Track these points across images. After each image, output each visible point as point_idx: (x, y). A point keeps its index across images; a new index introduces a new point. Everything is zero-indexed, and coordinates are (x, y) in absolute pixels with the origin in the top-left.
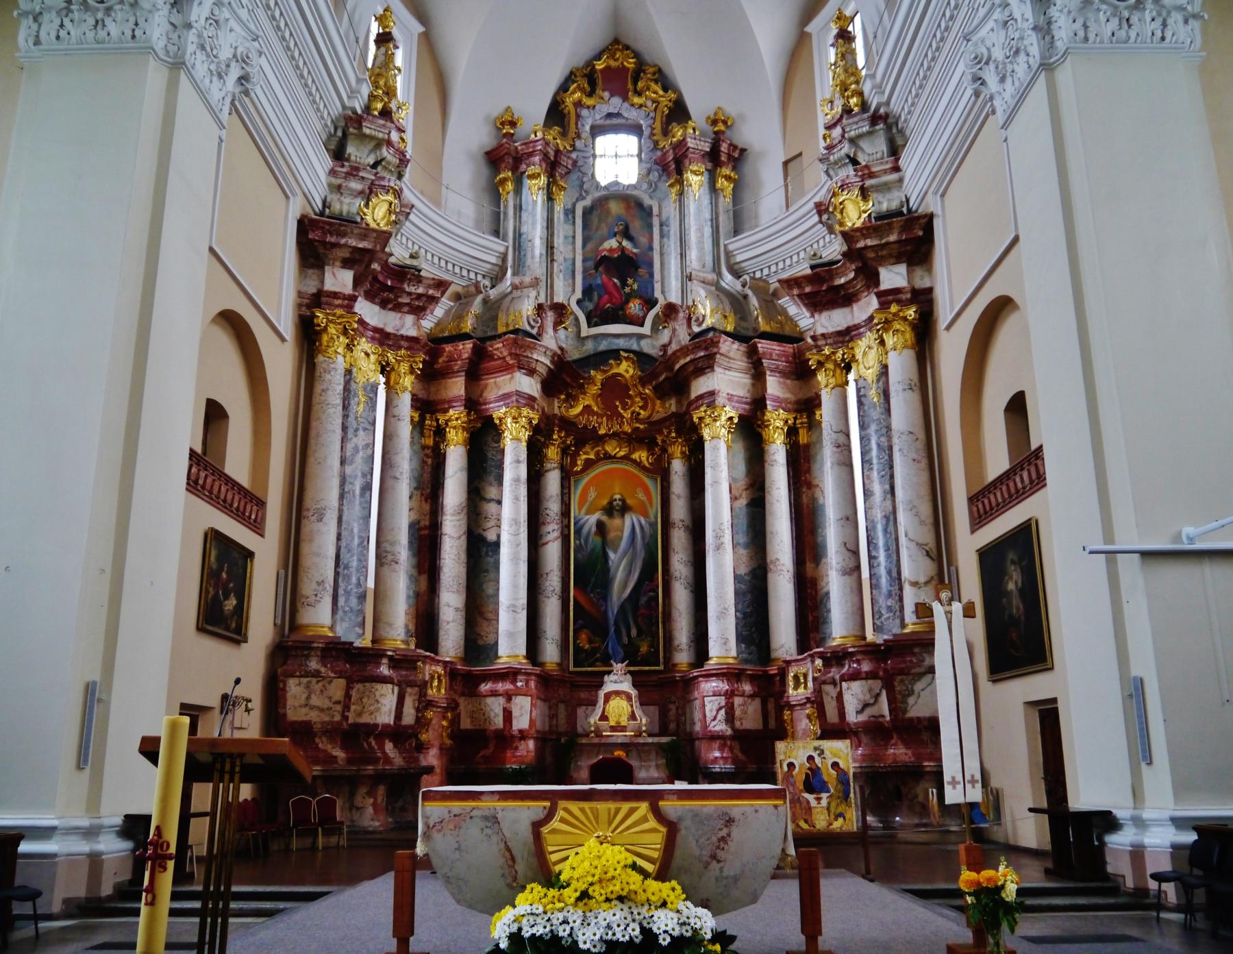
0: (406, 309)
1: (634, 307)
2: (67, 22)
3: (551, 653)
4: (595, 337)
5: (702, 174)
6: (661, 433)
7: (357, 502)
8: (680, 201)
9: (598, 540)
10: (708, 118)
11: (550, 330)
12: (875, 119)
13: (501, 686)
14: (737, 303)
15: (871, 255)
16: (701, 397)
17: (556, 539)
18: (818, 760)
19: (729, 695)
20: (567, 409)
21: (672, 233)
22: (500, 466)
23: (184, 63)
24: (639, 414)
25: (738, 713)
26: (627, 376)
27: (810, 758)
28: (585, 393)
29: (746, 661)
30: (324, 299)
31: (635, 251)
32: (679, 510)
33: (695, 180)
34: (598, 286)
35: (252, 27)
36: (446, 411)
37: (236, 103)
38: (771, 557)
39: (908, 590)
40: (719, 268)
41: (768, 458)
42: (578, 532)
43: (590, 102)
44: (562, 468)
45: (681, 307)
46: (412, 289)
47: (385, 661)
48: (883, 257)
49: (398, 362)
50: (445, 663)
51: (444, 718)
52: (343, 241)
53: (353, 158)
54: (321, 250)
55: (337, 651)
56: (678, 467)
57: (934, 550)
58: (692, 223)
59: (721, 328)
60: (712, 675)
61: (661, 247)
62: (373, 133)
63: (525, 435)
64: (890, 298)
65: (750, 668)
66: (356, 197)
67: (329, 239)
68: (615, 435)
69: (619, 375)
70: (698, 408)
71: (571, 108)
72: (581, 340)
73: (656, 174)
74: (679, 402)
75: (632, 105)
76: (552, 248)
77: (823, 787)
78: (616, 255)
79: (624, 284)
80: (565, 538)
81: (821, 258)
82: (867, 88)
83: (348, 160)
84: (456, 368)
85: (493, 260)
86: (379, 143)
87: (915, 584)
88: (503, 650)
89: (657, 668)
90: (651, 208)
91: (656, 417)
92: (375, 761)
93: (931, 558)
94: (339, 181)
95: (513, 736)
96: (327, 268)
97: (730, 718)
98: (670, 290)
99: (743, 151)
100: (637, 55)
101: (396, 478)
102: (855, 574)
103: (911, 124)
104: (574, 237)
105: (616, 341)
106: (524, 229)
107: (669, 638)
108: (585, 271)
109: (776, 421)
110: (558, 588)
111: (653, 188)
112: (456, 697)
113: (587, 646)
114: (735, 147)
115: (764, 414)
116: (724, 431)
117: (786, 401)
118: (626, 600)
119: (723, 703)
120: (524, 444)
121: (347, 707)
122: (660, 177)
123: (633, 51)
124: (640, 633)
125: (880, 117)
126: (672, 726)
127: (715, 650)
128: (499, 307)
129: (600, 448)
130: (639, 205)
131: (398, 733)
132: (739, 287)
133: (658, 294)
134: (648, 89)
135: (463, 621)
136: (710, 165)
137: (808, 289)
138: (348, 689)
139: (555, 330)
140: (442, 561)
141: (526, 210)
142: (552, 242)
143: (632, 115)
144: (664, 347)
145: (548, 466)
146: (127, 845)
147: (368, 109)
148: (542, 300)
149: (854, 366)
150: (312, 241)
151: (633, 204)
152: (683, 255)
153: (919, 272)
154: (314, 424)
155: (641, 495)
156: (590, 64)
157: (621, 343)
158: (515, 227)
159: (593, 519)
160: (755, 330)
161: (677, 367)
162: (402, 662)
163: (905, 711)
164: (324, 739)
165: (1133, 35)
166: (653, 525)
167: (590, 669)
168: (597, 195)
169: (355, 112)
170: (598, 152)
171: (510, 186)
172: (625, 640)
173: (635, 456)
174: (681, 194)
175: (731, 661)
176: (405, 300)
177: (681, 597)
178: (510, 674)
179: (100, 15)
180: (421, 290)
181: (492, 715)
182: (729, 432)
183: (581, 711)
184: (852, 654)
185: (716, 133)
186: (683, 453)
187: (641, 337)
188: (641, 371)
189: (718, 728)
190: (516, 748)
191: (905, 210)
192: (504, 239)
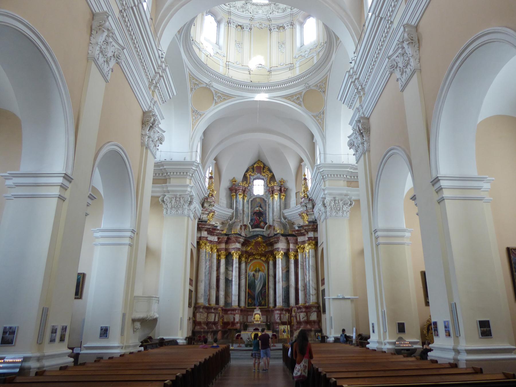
0: (215, 235)
1: (262, 224)
2: (172, 210)
3: (243, 304)
4: (253, 231)
5: (277, 195)
6: (267, 255)
7: (207, 277)
8: (273, 200)
9: (253, 278)
10: (280, 181)
11: (243, 230)
12: (309, 200)
13: (232, 312)
14: (284, 226)
15: (307, 230)
16: (276, 249)
17: (244, 278)
18: (285, 328)
19: (280, 314)
20: (247, 249)
21: (271, 207)
22: (232, 263)
23: (190, 216)
24: (263, 249)
25: (282, 318)
26: (260, 241)
27: (284, 328)
28: (251, 245)
29: (284, 306)
30: (202, 238)
31: (262, 211)
32: (271, 272)
33: (276, 197)
34: (254, 219)
35: (197, 201)
36: (221, 251)
37: (194, 216)
38: (290, 284)
39: (311, 296)
40: (281, 217)
41: (290, 262)
42: (249, 276)
43: (253, 174)
44: (245, 262)
45: (272, 225)
46: (217, 232)
47: (213, 309)
48: (309, 230)
49: (214, 247)
50: (221, 308)
51: (221, 319)
52: (205, 227)
53: (206, 207)
54: (201, 228)
55: (205, 308)
56: (271, 262)
57: (316, 288)
58: (275, 206)
59: (281, 233)
60: (277, 310)
61: (268, 210)
62: (210, 201)
63: (238, 257)
64: (310, 239)
65: (285, 308)
66: (206, 214)
67: (203, 226)
68: (257, 254)
69: (258, 241)
70: (275, 251)
71: (248, 176)
72: (250, 232)
73: (267, 193)
74: (271, 248)
75: (262, 175)
76: (244, 211)
77: (285, 332)
78: (258, 212)
79: (260, 218)
80: (246, 278)
81: (300, 225)
82: (308, 194)
83: (205, 207)
84: (223, 242)
85: (231, 214)
86: (211, 202)
87: (312, 295)
88: (233, 304)
89: (265, 307)
90: (266, 201)
91: (266, 251)
92: (211, 329)
93: (316, 290)
94: (203, 212)
95: (235, 323)
96: (202, 232)
97: (280, 319)
98: (270, 221)
99: (287, 189)
100: (264, 164)
101: (214, 271)
102: (304, 291)
103: (316, 202)
104: (249, 208)
105: (258, 232)
106: (237, 207)
107: (268, 301)
108: (251, 215)
109: (292, 254)
110: (244, 290)
111: (267, 196)
112: (223, 315)
113: (250, 302)
114: (285, 188)
115: (289, 252)
116: (280, 257)
117: (294, 249)
118: (259, 292)
119: (279, 316)
120: (238, 259)
121: (207, 318)
122: (268, 193)
123: (263, 163)
124: (262, 299)
125: (310, 200)
126: (269, 321)
127: (278, 304)
128: (232, 226)
129: (254, 257)
130: (264, 200)
131: (215, 323)
132: (285, 222)
133: (267, 222)
134: (266, 172)
135: (224, 298)
136: (279, 192)
137: (296, 232)
138: (207, 315)
139: (244, 230)
140: (220, 285)
141: (238, 202)
142: (244, 209)
143: (263, 177)
144: (269, 234)
145: (242, 262)
146: (186, 341)
147: (208, 195)
148: (241, 224)
149: (305, 249)
150: (200, 227)
151: (262, 199)
152: (273, 213)
153: (316, 233)
154: (200, 263)
155: (263, 267)
156: (253, 165)
157: (259, 233)
158: (235, 206)
159: (252, 273)
160: (288, 233)
161: (271, 241)
162: (215, 309)
163: (309, 319)
164: (203, 324)
165: (338, 215)
166: (265, 275)
167: (251, 307)
168: (254, 197)
169: (206, 197)
170: (254, 184)
171: (235, 197)
172: (259, 301)
173: (262, 258)
174: (273, 199)
175: (281, 307)
176: (215, 234)
177: (271, 292)
178: (234, 310)
179: (177, 209)
180: (218, 232)
181: (231, 318)
182: (282, 256)
183: (249, 317)
184: (302, 308)
185: (281, 184)
186: (272, 259)
187: (263, 231)
188: (264, 240)
189: (278, 321)
190: (236, 326)
191: (314, 220)
192: (233, 209)
